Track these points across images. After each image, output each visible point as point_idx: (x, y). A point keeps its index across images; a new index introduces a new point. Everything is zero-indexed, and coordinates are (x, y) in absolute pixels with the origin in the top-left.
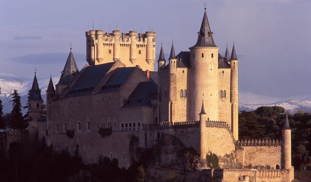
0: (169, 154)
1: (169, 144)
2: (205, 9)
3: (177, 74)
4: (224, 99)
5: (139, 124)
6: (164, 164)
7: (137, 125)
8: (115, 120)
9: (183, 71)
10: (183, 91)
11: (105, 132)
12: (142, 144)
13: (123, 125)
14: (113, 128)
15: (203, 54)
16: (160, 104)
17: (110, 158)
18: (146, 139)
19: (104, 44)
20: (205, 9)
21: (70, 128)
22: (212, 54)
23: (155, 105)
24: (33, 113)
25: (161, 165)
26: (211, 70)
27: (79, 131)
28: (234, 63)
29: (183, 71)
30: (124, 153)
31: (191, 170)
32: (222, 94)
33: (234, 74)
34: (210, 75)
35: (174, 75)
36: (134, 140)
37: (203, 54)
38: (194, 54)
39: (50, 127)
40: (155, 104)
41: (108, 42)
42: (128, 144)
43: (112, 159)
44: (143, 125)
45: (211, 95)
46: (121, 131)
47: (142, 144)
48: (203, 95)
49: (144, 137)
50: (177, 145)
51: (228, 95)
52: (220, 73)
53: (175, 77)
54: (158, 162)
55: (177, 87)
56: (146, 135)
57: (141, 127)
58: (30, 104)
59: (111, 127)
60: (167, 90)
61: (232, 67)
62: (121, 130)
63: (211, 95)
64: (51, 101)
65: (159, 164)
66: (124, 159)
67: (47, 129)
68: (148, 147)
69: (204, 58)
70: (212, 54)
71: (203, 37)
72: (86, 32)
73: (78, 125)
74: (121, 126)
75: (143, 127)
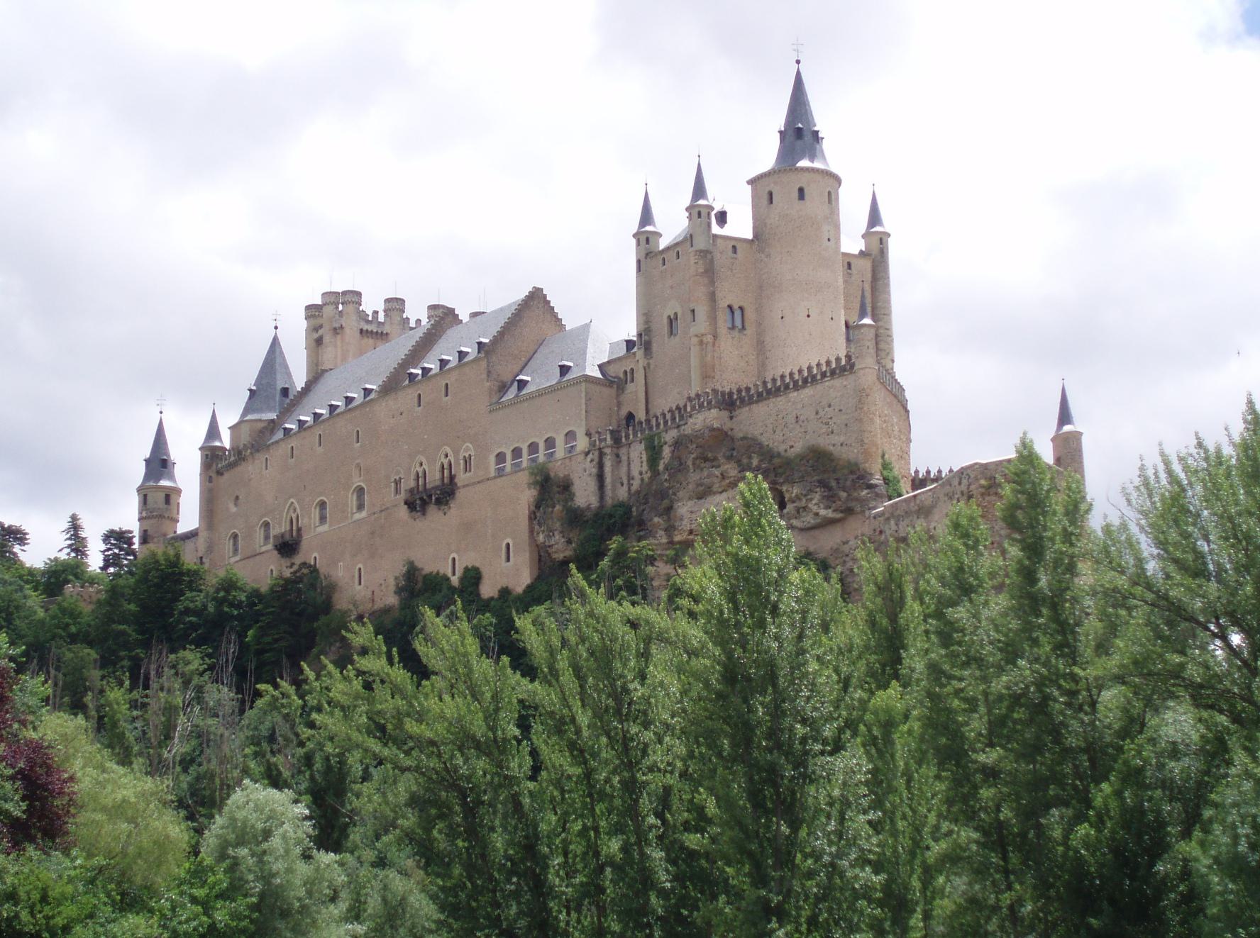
0: (715, 493)
1: (715, 459)
2: (798, 62)
3: (717, 256)
5: (570, 435)
6: (691, 532)
7: (560, 441)
8: (467, 449)
10: (733, 312)
11: (429, 498)
12: (585, 495)
13: (500, 458)
14: (461, 478)
15: (801, 190)
16: (649, 364)
17: (449, 574)
18: (600, 477)
19: (361, 331)
20: (798, 62)
23: (622, 376)
24: (153, 521)
25: (677, 538)
27: (321, 529)
30: (508, 545)
31: (829, 513)
35: (709, 256)
36: (550, 488)
37: (801, 190)
38: (771, 194)
39: (210, 548)
40: (625, 372)
41: (370, 328)
42: (524, 512)
43: (454, 574)
44: (588, 434)
46: (495, 478)
47: (585, 495)
49: (594, 471)
50: (750, 458)
53: (712, 261)
54: (661, 533)
55: (719, 294)
56: (601, 466)
57: (582, 443)
58: (145, 496)
59: (452, 478)
60: (676, 314)
62: (493, 474)
64: (214, 475)
65: (670, 536)
66: (508, 560)
67: (200, 554)
68: (609, 501)
71: (799, 143)
72: (308, 308)
73: (316, 514)
74: (492, 459)
75: (587, 439)
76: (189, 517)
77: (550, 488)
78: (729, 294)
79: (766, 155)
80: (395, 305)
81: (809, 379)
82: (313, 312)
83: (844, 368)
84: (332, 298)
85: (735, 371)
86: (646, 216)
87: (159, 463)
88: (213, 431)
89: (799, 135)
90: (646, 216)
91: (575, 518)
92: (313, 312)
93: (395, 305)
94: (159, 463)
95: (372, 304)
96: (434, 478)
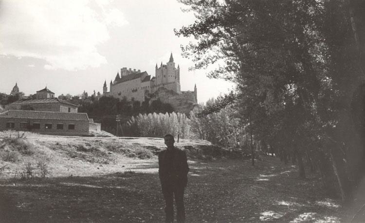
11: (134, 91)
12: (150, 92)
21: (119, 93)
36: (147, 91)
76: (108, 90)
77: (147, 91)
78: (164, 74)
79: (168, 60)
80: (130, 69)
81: (171, 83)
82: (121, 69)
83: (174, 83)
84: (124, 68)
85: (164, 82)
86: (157, 66)
87: (105, 85)
88: (111, 82)
89: (171, 59)
90: (157, 66)
91: (149, 94)
92: (121, 69)
93: (130, 69)
94: (105, 85)
95: (128, 69)
96: (135, 89)
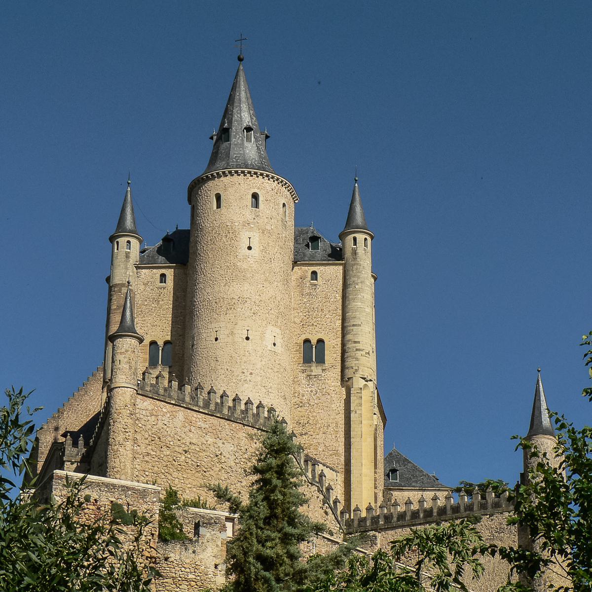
4: (316, 370)
9: (163, 276)
22: (255, 196)
26: (250, 248)
28: (355, 239)
29: (163, 276)
32: (312, 352)
33: (353, 279)
34: (245, 266)
37: (218, 197)
45: (247, 338)
48: (216, 339)
51: (332, 355)
52: (302, 278)
61: (348, 254)
63: (247, 338)
69: (223, 209)
70: (255, 196)
